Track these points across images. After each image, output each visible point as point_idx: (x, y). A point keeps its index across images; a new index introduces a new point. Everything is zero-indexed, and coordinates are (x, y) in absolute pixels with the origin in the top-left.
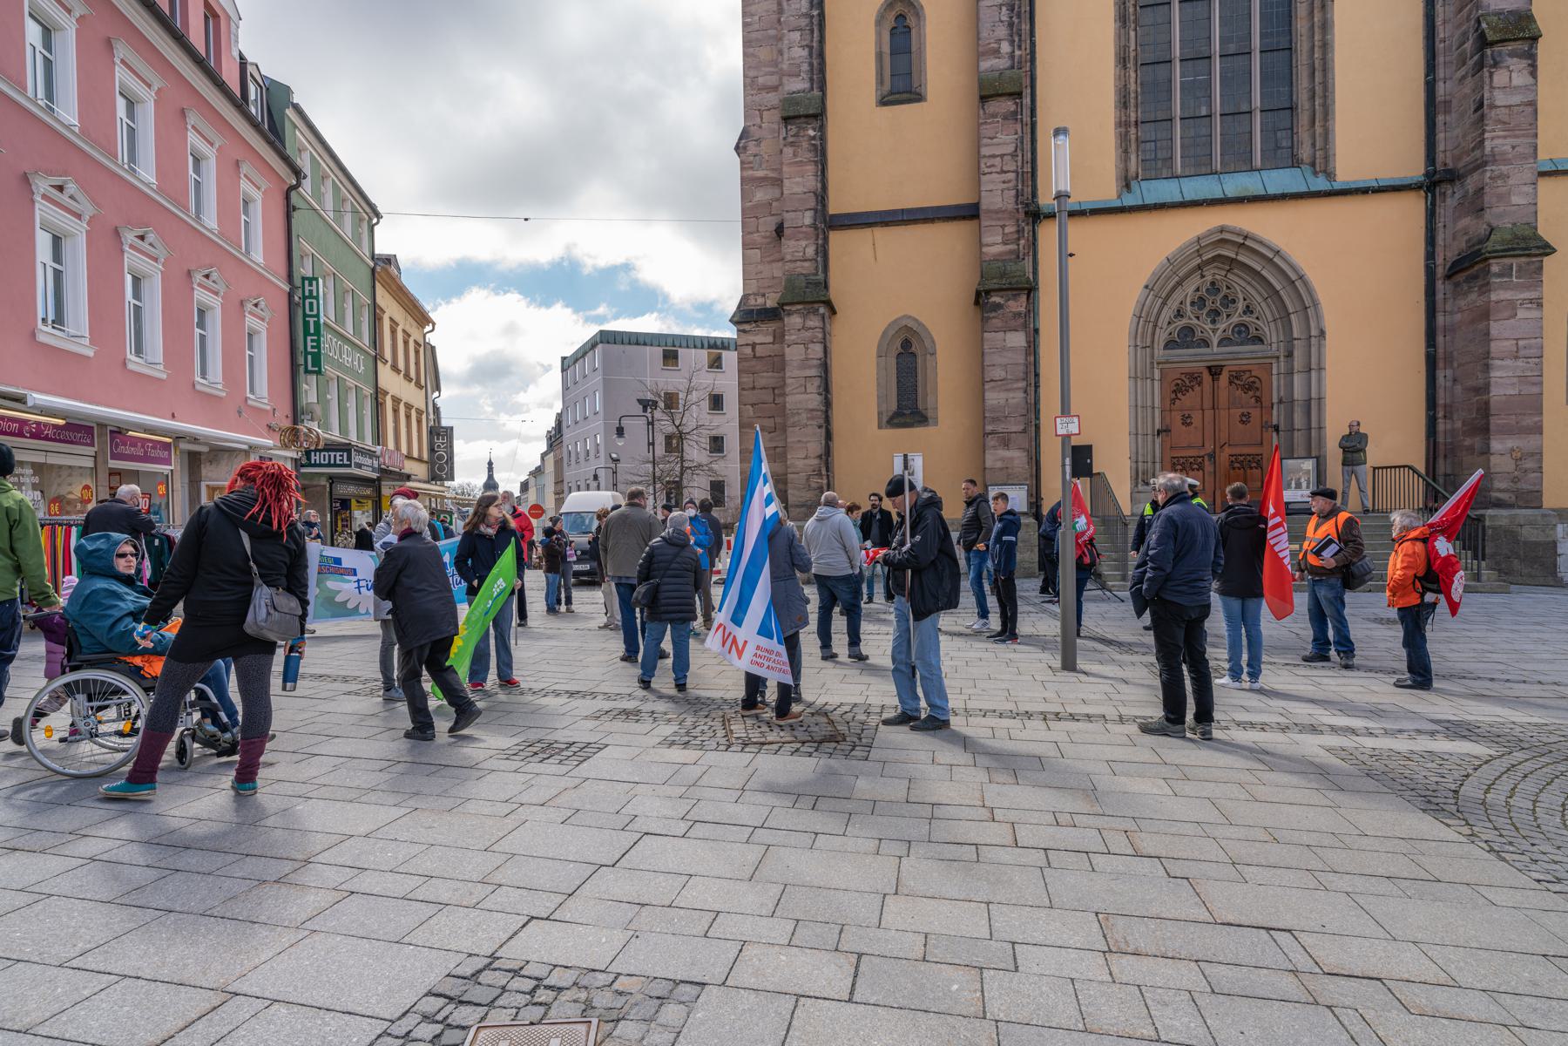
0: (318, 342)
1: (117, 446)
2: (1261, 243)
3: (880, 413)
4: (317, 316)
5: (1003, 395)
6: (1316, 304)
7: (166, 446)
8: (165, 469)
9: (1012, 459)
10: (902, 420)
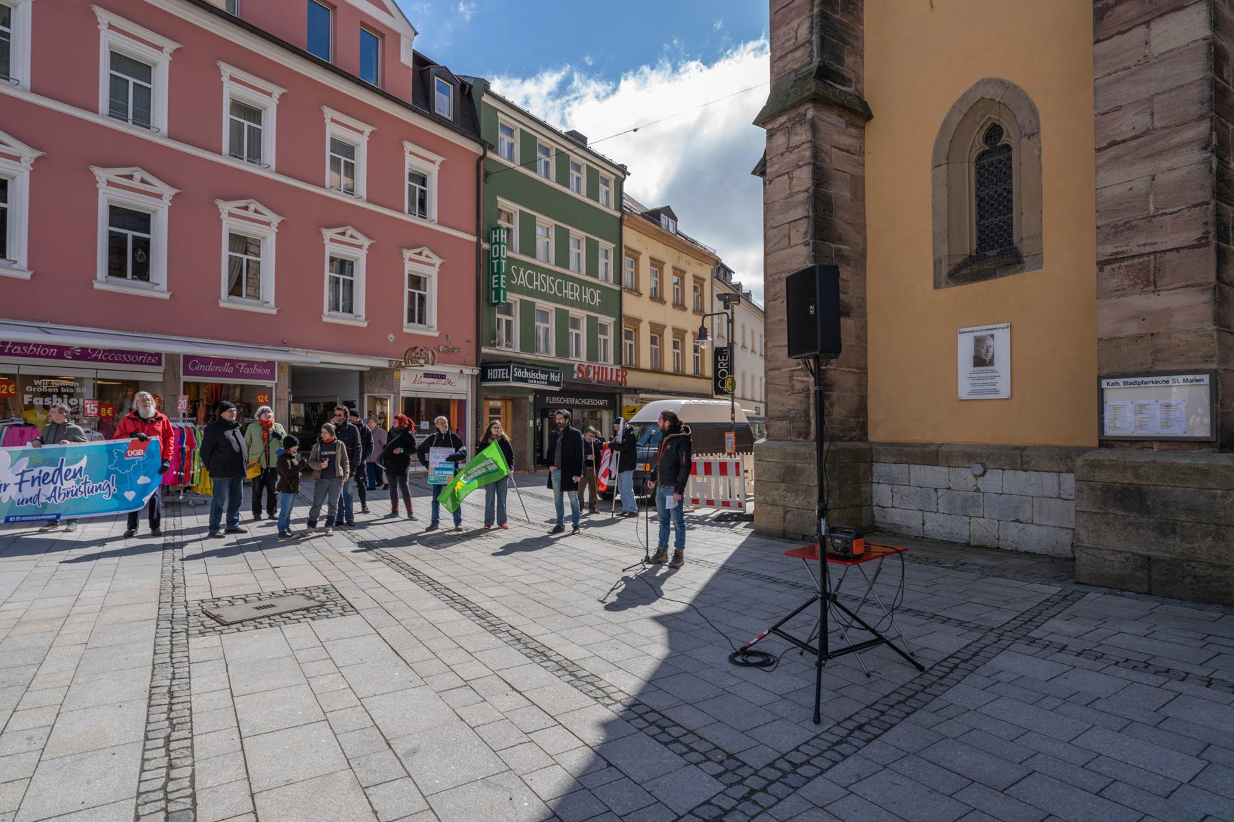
0: (499, 279)
1: (194, 365)
3: (937, 263)
4: (499, 258)
7: (270, 364)
8: (269, 383)
9: (1167, 312)
10: (975, 268)
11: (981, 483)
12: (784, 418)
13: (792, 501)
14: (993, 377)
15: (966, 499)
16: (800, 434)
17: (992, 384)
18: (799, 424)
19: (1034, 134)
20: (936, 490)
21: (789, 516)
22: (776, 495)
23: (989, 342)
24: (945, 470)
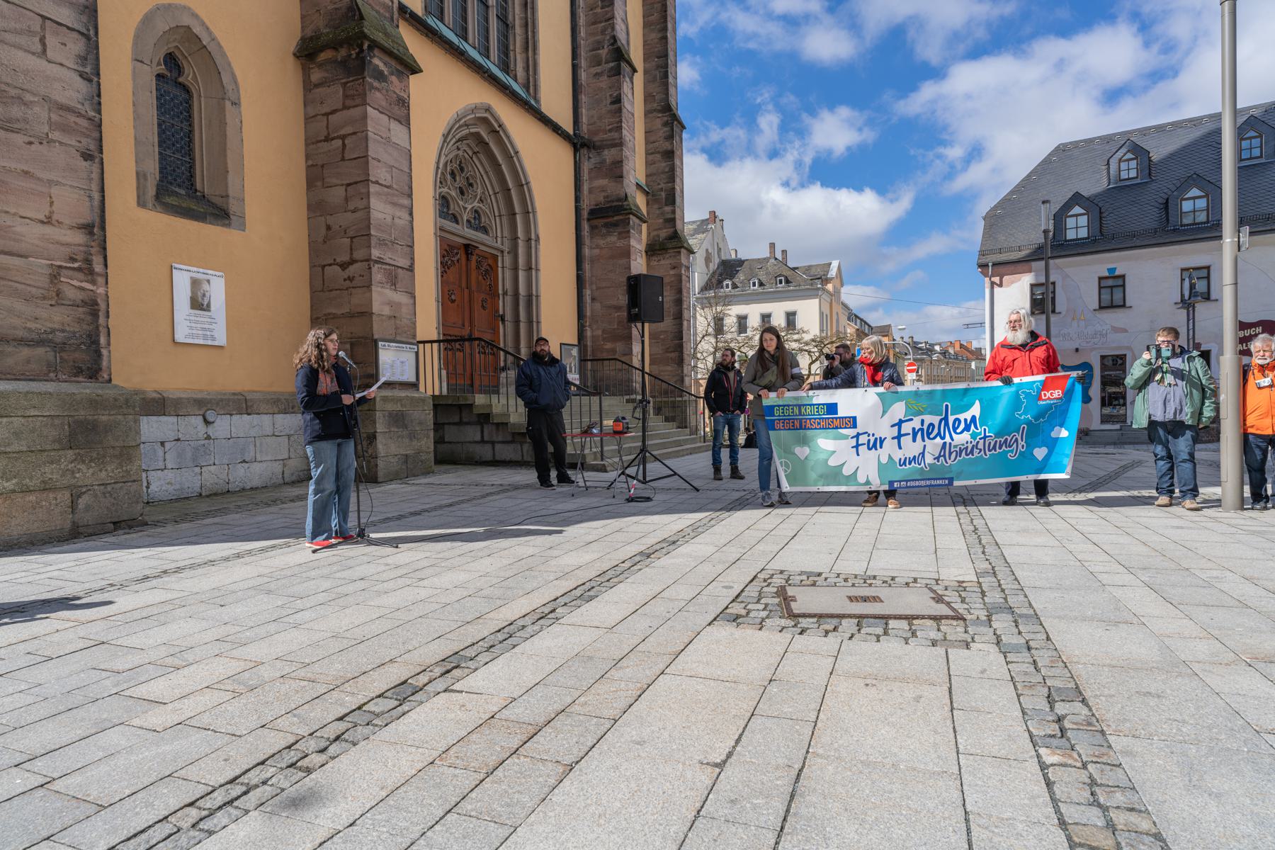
2: (508, 137)
3: (141, 176)
5: (389, 210)
6: (534, 212)
9: (400, 304)
11: (211, 431)
12: (40, 343)
13: (87, 474)
14: (211, 323)
15: (197, 449)
16: (78, 371)
17: (210, 330)
18: (77, 355)
19: (236, 104)
20: (162, 444)
21: (82, 502)
22: (51, 472)
23: (205, 286)
24: (174, 419)
